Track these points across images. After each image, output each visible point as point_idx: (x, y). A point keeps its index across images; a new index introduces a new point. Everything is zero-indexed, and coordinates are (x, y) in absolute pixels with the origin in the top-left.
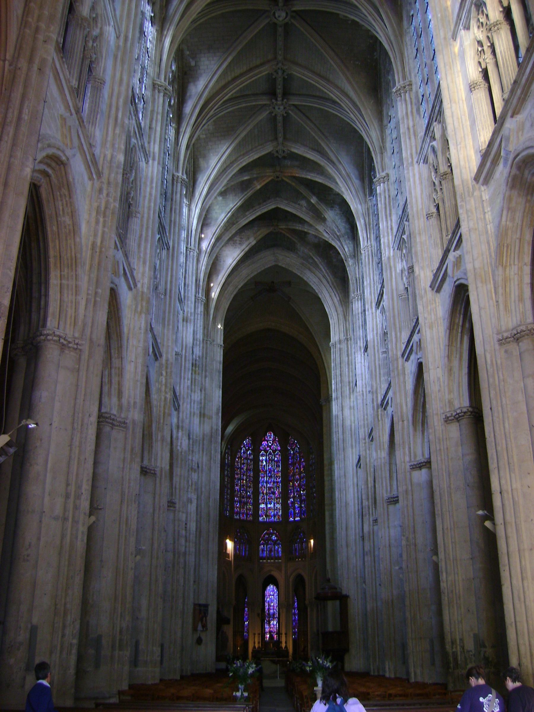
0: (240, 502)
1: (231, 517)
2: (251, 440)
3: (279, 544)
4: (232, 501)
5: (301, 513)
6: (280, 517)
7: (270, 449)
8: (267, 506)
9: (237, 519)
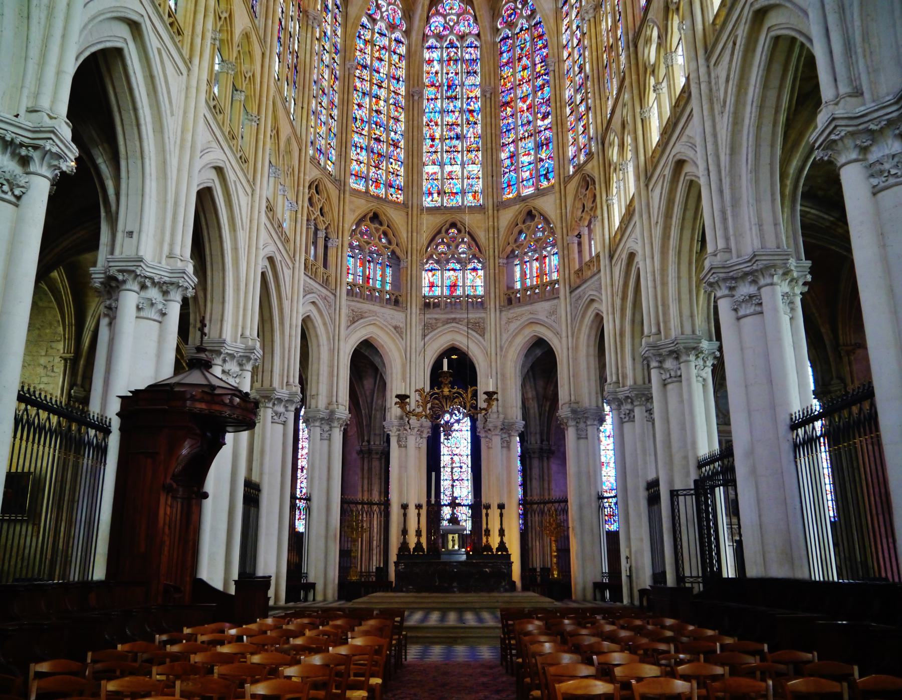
0: (369, 150)
1: (341, 184)
2: (404, 12)
3: (475, 269)
4: (344, 146)
5: (537, 177)
7: (451, 32)
8: (442, 165)
9: (356, 192)
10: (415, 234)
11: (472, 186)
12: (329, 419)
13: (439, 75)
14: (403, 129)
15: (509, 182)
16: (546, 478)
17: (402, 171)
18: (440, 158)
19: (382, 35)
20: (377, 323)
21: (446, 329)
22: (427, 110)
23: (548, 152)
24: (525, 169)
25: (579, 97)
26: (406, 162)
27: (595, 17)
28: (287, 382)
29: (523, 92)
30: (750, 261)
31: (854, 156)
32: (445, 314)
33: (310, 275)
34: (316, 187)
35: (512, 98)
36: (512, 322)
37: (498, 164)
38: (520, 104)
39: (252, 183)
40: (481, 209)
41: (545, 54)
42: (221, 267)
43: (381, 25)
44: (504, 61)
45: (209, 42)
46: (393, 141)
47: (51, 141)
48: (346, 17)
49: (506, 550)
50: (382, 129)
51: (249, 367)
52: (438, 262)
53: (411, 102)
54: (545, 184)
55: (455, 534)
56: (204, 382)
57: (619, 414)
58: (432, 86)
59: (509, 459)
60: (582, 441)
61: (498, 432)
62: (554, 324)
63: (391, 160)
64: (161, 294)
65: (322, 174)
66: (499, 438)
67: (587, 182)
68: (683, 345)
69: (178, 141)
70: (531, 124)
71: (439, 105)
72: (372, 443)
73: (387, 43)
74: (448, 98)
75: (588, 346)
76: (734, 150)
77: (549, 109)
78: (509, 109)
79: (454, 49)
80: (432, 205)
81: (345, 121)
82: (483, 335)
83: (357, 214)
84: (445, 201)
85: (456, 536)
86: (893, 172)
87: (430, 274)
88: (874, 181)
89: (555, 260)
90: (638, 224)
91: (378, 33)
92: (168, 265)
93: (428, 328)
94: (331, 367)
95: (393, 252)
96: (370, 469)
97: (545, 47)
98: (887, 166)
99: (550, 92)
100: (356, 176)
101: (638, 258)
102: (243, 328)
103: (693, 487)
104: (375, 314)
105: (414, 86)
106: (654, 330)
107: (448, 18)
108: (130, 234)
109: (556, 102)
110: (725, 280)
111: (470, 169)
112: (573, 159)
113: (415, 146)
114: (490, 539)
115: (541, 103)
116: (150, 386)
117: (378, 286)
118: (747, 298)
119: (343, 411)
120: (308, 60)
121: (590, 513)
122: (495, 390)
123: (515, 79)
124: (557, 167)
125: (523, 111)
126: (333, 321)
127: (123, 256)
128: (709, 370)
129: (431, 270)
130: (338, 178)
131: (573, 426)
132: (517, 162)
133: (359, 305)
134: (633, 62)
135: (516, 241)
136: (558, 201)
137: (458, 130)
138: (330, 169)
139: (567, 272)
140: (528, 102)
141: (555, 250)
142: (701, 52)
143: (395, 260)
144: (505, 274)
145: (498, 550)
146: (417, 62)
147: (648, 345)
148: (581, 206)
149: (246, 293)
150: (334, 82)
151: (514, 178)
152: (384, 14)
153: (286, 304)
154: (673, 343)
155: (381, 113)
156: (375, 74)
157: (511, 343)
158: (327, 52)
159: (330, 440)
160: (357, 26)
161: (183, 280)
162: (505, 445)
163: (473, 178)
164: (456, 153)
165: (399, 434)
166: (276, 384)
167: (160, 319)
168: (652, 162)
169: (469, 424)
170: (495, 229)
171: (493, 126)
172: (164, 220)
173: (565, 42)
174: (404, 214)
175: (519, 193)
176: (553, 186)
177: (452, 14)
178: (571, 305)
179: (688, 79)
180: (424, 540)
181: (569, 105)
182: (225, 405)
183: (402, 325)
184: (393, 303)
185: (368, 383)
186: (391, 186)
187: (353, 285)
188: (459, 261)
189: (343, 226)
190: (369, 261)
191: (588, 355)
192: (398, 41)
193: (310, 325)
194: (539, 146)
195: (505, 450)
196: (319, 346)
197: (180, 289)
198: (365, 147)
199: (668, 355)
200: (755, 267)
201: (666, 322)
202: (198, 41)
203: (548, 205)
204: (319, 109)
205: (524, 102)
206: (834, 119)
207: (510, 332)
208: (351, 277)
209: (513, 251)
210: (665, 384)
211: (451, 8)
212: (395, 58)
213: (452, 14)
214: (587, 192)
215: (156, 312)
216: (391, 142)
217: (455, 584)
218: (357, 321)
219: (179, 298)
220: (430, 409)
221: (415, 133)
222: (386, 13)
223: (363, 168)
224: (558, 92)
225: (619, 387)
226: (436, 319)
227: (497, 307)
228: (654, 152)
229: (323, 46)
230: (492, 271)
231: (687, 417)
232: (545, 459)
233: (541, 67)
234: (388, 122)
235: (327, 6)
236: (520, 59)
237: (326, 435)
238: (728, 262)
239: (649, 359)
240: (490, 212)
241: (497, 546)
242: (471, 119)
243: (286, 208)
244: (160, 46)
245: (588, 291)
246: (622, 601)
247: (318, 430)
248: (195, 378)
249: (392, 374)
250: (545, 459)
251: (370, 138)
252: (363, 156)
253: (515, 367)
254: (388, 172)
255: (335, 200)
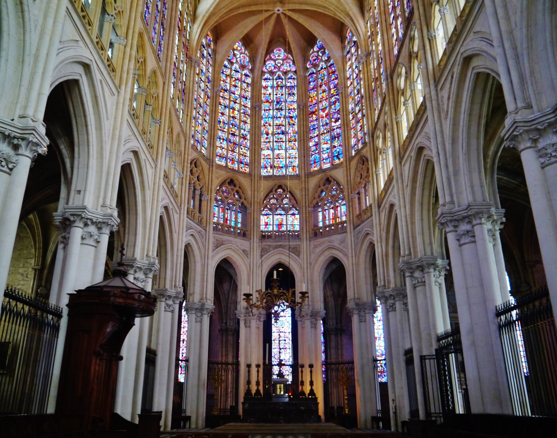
0: (228, 140)
1: (210, 161)
3: (293, 214)
4: (213, 138)
5: (332, 157)
6: (297, 169)
7: (279, 70)
8: (273, 150)
9: (220, 166)
10: (256, 192)
11: (292, 162)
12: (201, 309)
13: (272, 95)
14: (249, 128)
15: (315, 160)
16: (340, 347)
17: (248, 154)
18: (272, 145)
19: (237, 71)
20: (232, 248)
21: (276, 251)
22: (264, 117)
23: (339, 142)
24: (324, 152)
25: (357, 109)
26: (251, 148)
27: (366, 61)
28: (175, 285)
29: (323, 106)
30: (466, 209)
31: (529, 145)
32: (275, 242)
33: (190, 217)
34: (195, 163)
35: (316, 109)
36: (317, 247)
37: (308, 149)
38: (321, 113)
39: (155, 161)
40: (297, 177)
41: (336, 83)
42: (134, 212)
43: (236, 66)
44: (311, 87)
45: (131, 76)
46: (243, 135)
47: (33, 135)
48: (215, 61)
49: (314, 395)
50: (236, 128)
51: (151, 275)
52: (270, 210)
53: (254, 112)
54: (337, 161)
55: (281, 384)
56: (122, 285)
57: (386, 306)
58: (267, 102)
59: (316, 335)
60: (363, 324)
61: (308, 317)
62: (344, 249)
63: (242, 147)
64: (97, 230)
65: (199, 155)
66: (309, 321)
67: (363, 160)
68: (425, 262)
69: (111, 136)
70: (328, 125)
71: (272, 114)
72: (228, 324)
73: (240, 76)
74: (277, 109)
75: (365, 262)
76: (454, 141)
77: (339, 116)
78: (314, 116)
79: (280, 80)
80: (267, 174)
81: (213, 123)
82: (298, 256)
83: (220, 180)
84: (275, 172)
85: (282, 385)
86: (554, 154)
87: (266, 217)
88: (542, 160)
89: (344, 209)
90: (395, 186)
91: (234, 70)
92: (102, 211)
93: (264, 251)
94: (203, 275)
95: (242, 204)
96: (227, 341)
97: (336, 78)
98: (549, 151)
99: (340, 106)
100: (220, 156)
101: (396, 208)
102: (148, 251)
103: (434, 353)
104: (230, 242)
105: (256, 102)
106: (407, 253)
107: (277, 62)
108: (79, 192)
109: (344, 111)
110: (451, 221)
111: (291, 152)
112: (354, 146)
113: (257, 138)
114: (304, 388)
115: (334, 112)
116: (88, 288)
117: (233, 224)
118: (466, 232)
119: (210, 304)
120: (191, 87)
121: (368, 369)
122: (306, 291)
123: (318, 98)
124: (344, 151)
125: (323, 117)
126: (204, 246)
127: (74, 205)
128: (443, 278)
129: (266, 215)
130: (208, 158)
131: (357, 314)
132: (320, 148)
133: (221, 237)
134: (390, 87)
135: (319, 196)
136: (345, 172)
137: (283, 128)
138: (204, 152)
139: (351, 216)
140: (326, 112)
141: (344, 202)
142: (432, 82)
143: (244, 209)
144: (313, 217)
145: (309, 394)
146: (258, 88)
147: (403, 262)
148: (359, 175)
149: (150, 229)
150: (207, 99)
151: (318, 158)
152: (238, 59)
153: (175, 236)
154: (419, 261)
155: (236, 118)
156: (233, 95)
157: (316, 260)
158: (203, 82)
159: (201, 322)
160: (221, 68)
161: (111, 220)
162: (313, 326)
163: (292, 158)
164: (281, 143)
165: (245, 319)
166: (168, 286)
167: (95, 245)
168: (403, 148)
169: (290, 312)
170: (306, 189)
171: (305, 126)
172: (100, 183)
173: (348, 76)
174: (249, 180)
175: (321, 167)
176: (342, 163)
177: (279, 59)
178: (354, 237)
179: (424, 98)
180: (261, 388)
181: (352, 114)
182: (135, 300)
183: (247, 249)
184: (242, 235)
185: (226, 286)
186: (241, 163)
187: (217, 224)
188: (284, 209)
189: (211, 188)
190: (227, 209)
191: (365, 269)
192: (246, 75)
193: (190, 249)
194: (333, 138)
195: (313, 329)
196: (195, 262)
197: (109, 226)
198: (225, 139)
199: (416, 268)
200: (470, 213)
201: (415, 247)
202: (125, 75)
203: (339, 175)
204: (197, 115)
205: (324, 111)
206: (515, 122)
207: (316, 254)
208: (216, 219)
209: (317, 203)
210: (415, 288)
211: (279, 56)
212: (245, 85)
213: (279, 59)
214: (364, 166)
215: (93, 241)
216: (242, 136)
217: (281, 418)
218: (220, 246)
219: (108, 232)
220: (265, 303)
221: (257, 131)
222: (240, 59)
223: (225, 152)
224: (344, 106)
225: (385, 289)
226: (269, 245)
227: (308, 238)
228: (404, 142)
229: (201, 78)
230: (304, 215)
231: (430, 309)
232: (339, 335)
233: (334, 91)
234: (240, 124)
235: (203, 55)
236: (321, 86)
237: (199, 319)
238: (452, 210)
239: (405, 271)
240: (303, 178)
241: (308, 392)
242: (291, 122)
243: (176, 176)
244: (101, 79)
245: (364, 227)
246: (390, 429)
247: (194, 316)
248: (117, 282)
249: (241, 280)
250: (339, 335)
251: (229, 133)
252: (224, 144)
253: (319, 276)
254: (239, 154)
255: (206, 171)
